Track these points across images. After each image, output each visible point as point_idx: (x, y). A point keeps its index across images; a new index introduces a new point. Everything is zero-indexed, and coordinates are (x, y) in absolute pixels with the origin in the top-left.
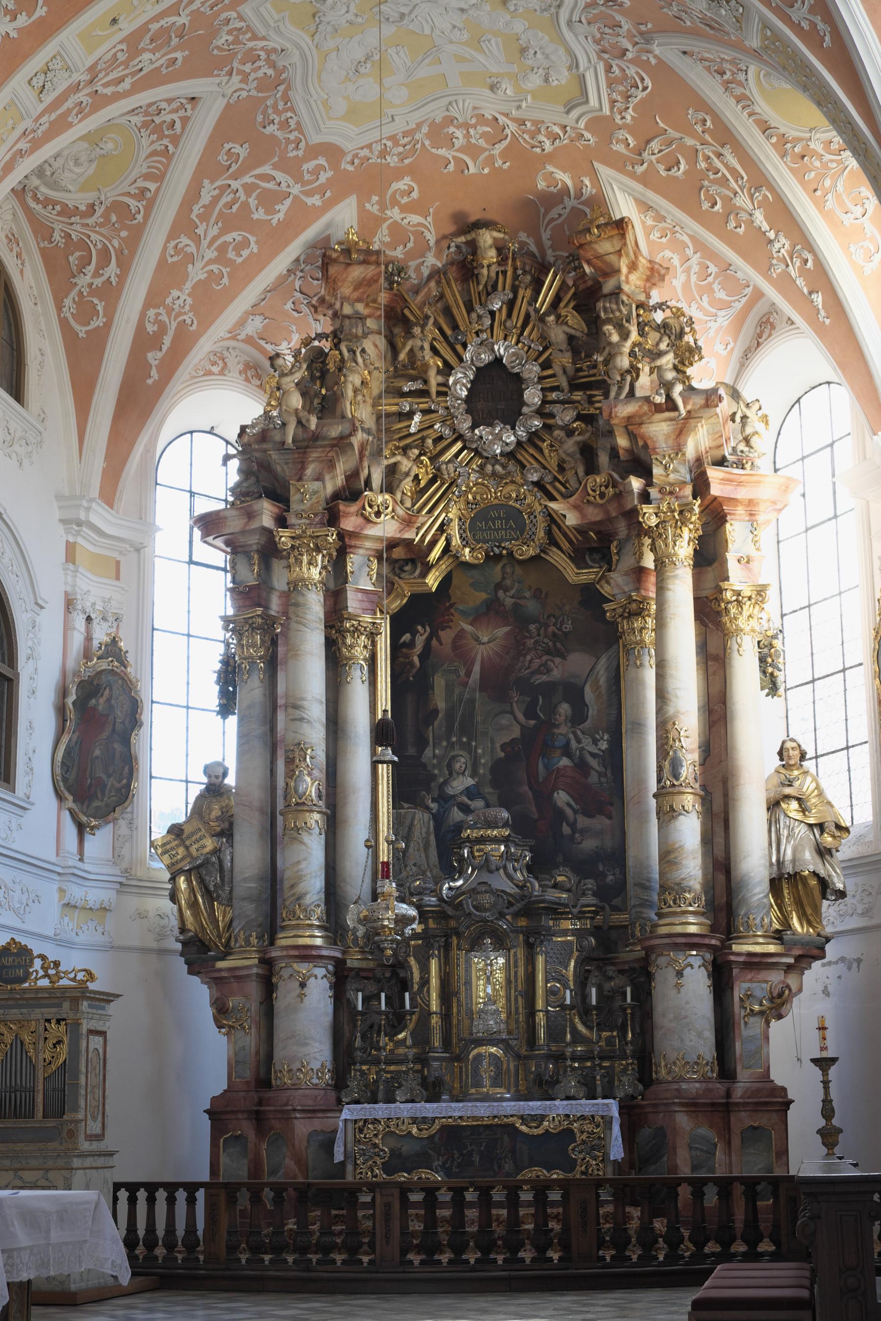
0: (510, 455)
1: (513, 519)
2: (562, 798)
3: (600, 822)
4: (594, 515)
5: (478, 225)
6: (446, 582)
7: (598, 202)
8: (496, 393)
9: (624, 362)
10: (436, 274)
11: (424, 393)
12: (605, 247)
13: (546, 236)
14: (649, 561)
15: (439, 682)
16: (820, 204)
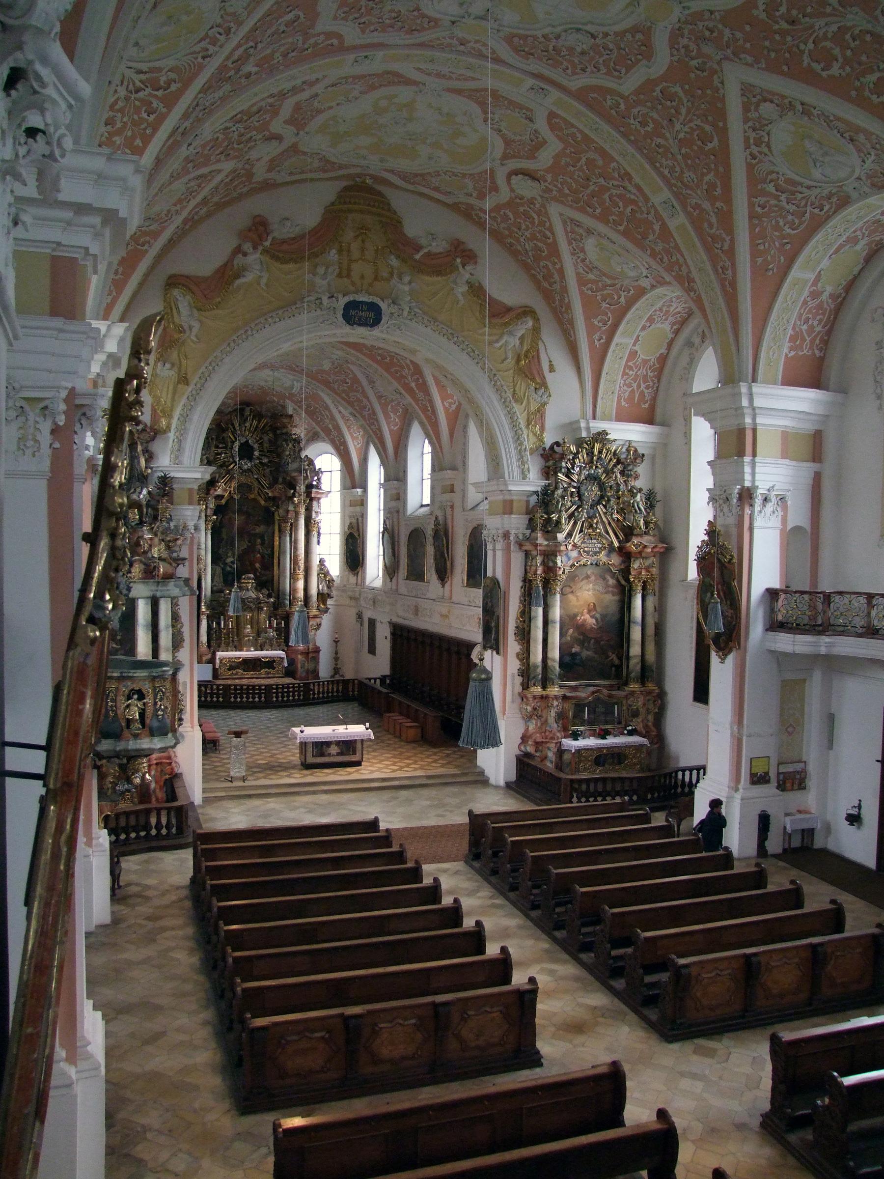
0: (249, 470)
1: (249, 488)
2: (257, 565)
3: (268, 573)
4: (276, 494)
5: (248, 404)
6: (227, 503)
7: (284, 407)
8: (246, 451)
9: (288, 453)
10: (230, 412)
11: (226, 448)
12: (285, 421)
13: (264, 409)
14: (291, 508)
15: (224, 530)
16: (349, 430)
